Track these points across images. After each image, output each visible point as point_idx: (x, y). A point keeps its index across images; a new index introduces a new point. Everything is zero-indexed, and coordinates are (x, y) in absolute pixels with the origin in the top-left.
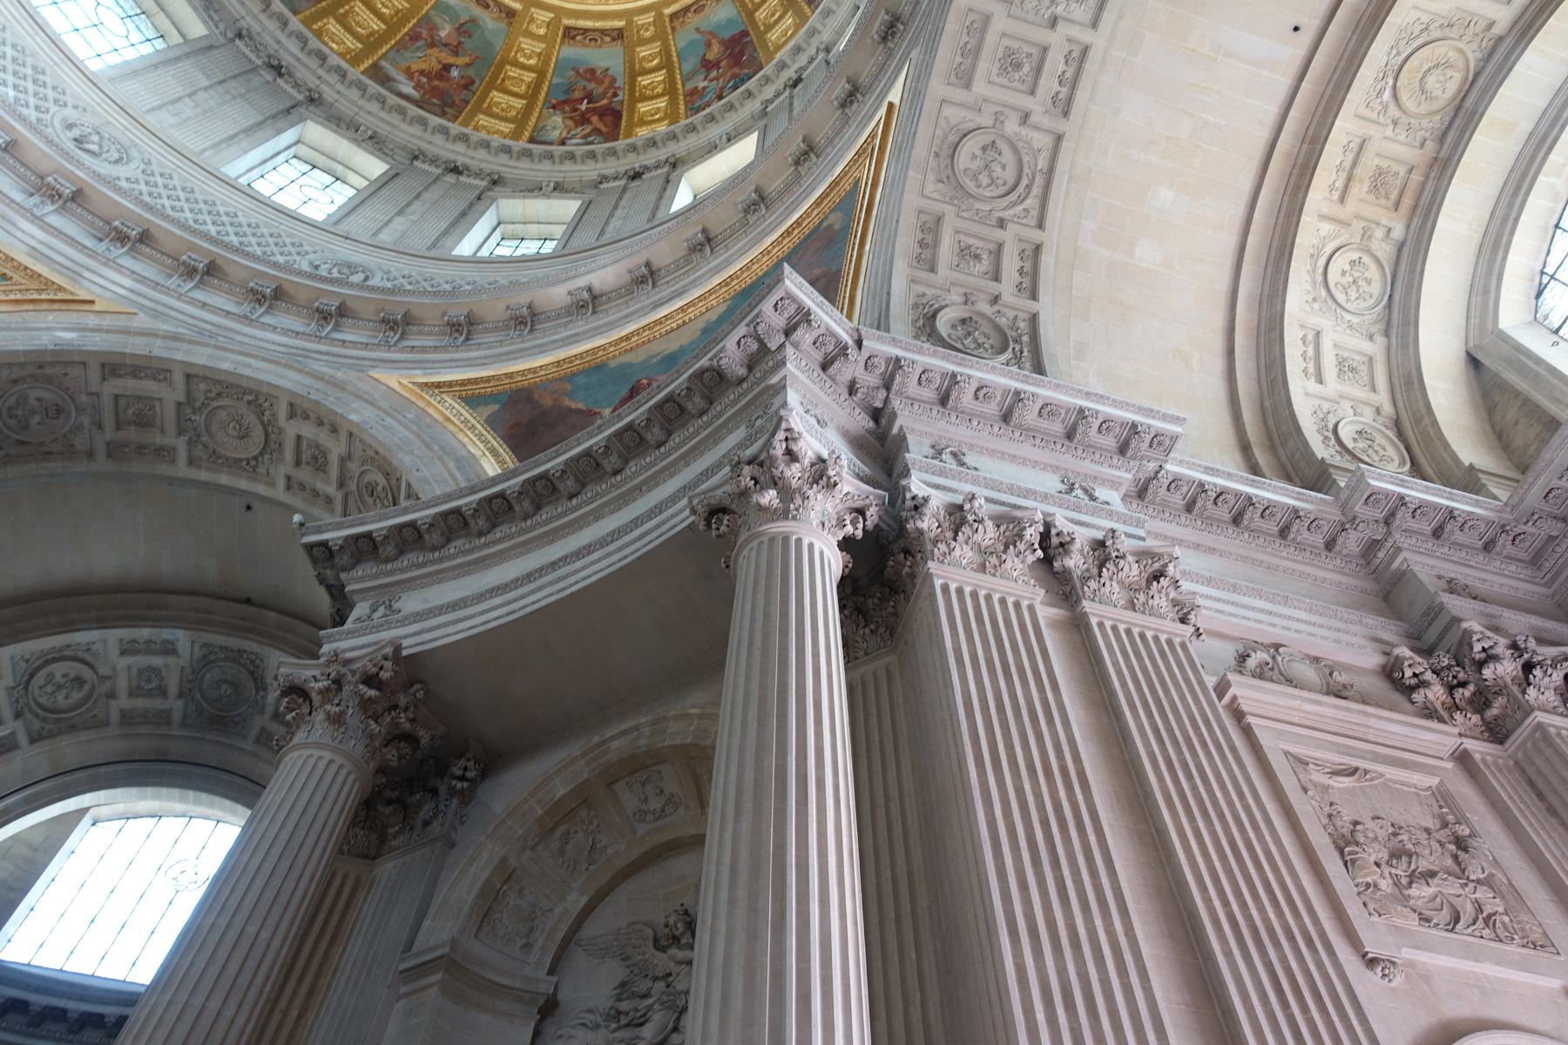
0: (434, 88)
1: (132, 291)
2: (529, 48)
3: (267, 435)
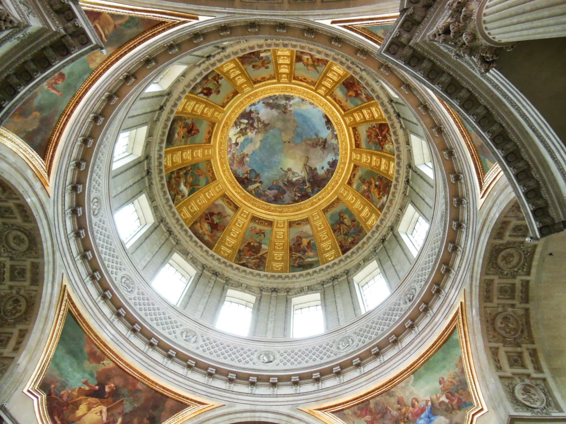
1: (456, 290)
3: (511, 248)
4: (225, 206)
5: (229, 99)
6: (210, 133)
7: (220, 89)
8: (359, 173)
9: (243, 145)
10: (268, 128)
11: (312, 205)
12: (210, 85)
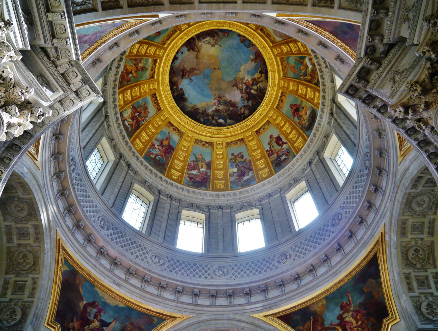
0: (124, 76)
2: (146, 88)
5: (263, 128)
6: (281, 101)
7: (268, 140)
8: (148, 73)
9: (256, 68)
10: (234, 83)
11: (189, 32)
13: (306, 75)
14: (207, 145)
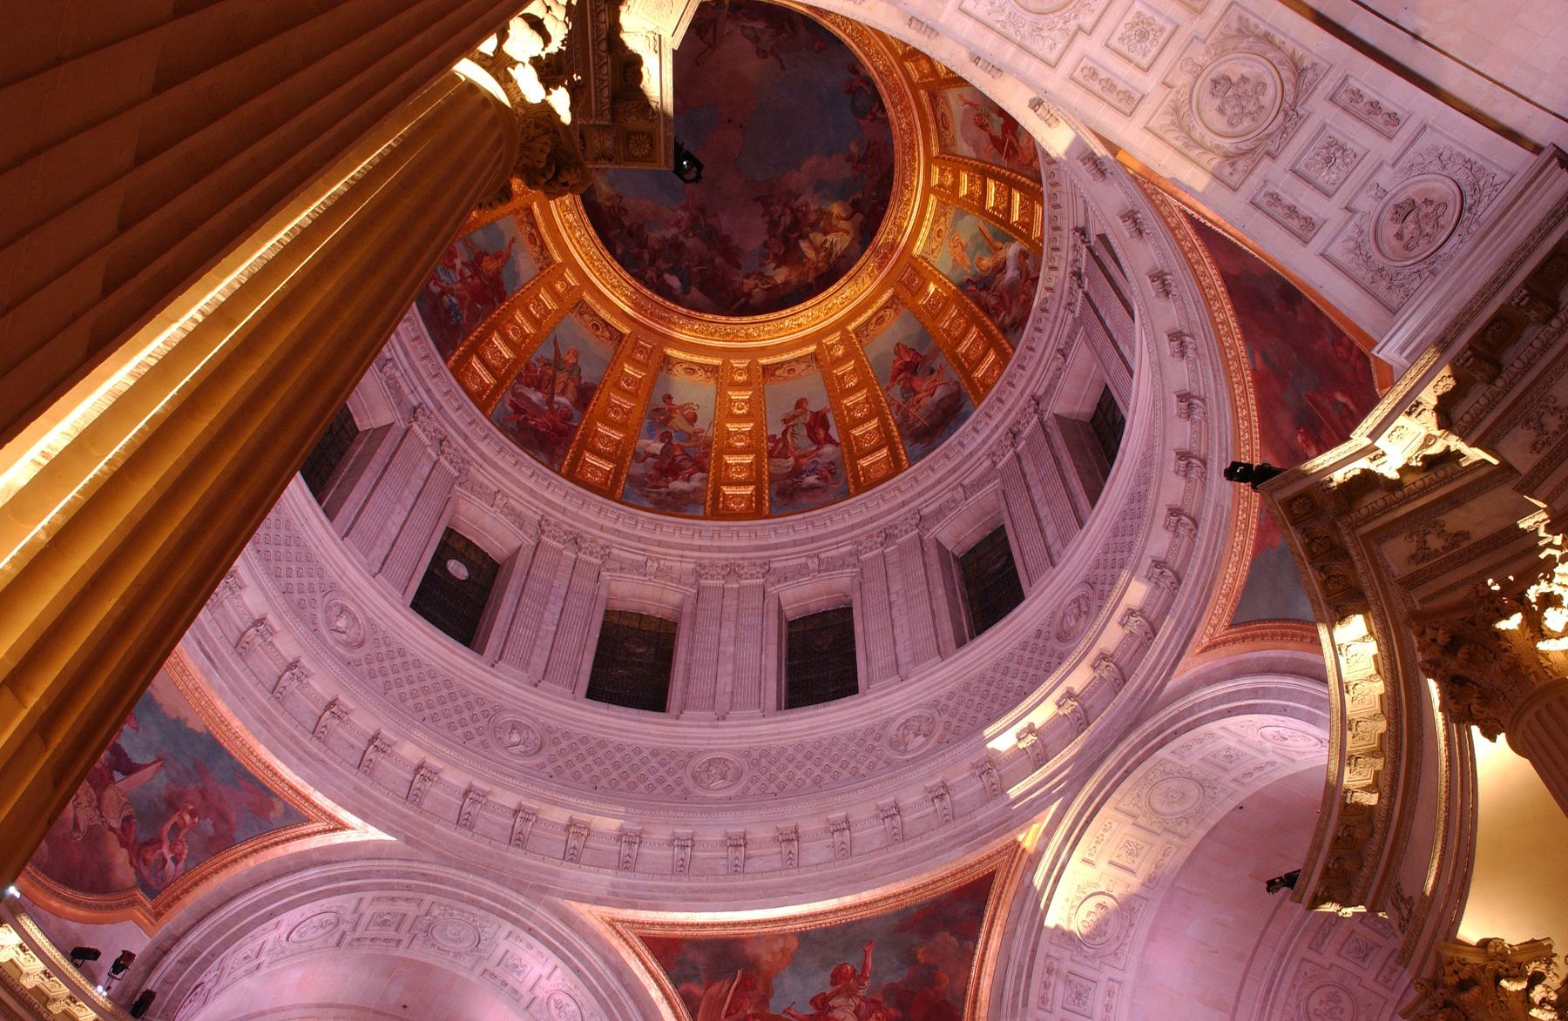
4: (958, 128)
7: (789, 409)
12: (802, 441)
13: (985, 288)
14: (607, 334)
